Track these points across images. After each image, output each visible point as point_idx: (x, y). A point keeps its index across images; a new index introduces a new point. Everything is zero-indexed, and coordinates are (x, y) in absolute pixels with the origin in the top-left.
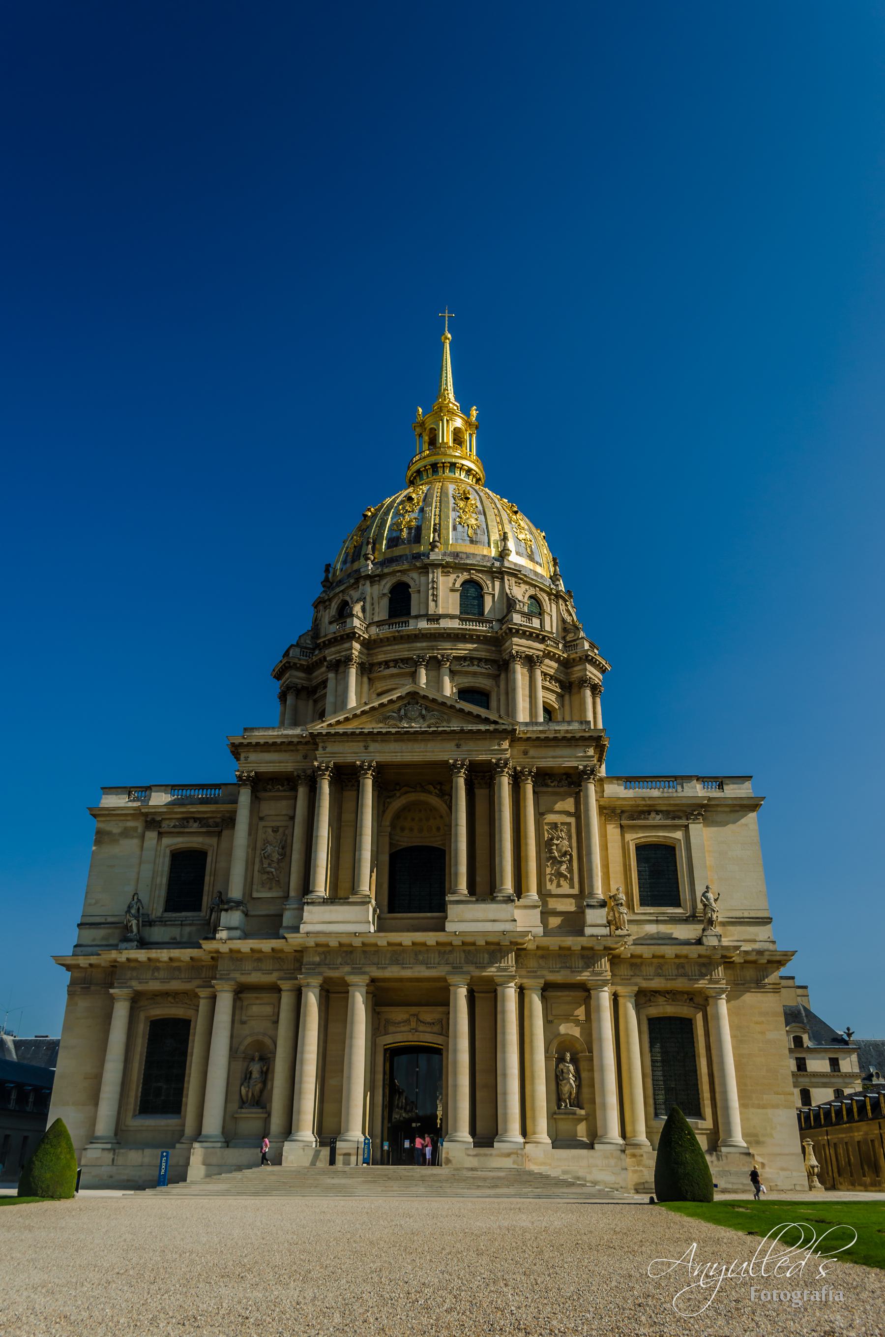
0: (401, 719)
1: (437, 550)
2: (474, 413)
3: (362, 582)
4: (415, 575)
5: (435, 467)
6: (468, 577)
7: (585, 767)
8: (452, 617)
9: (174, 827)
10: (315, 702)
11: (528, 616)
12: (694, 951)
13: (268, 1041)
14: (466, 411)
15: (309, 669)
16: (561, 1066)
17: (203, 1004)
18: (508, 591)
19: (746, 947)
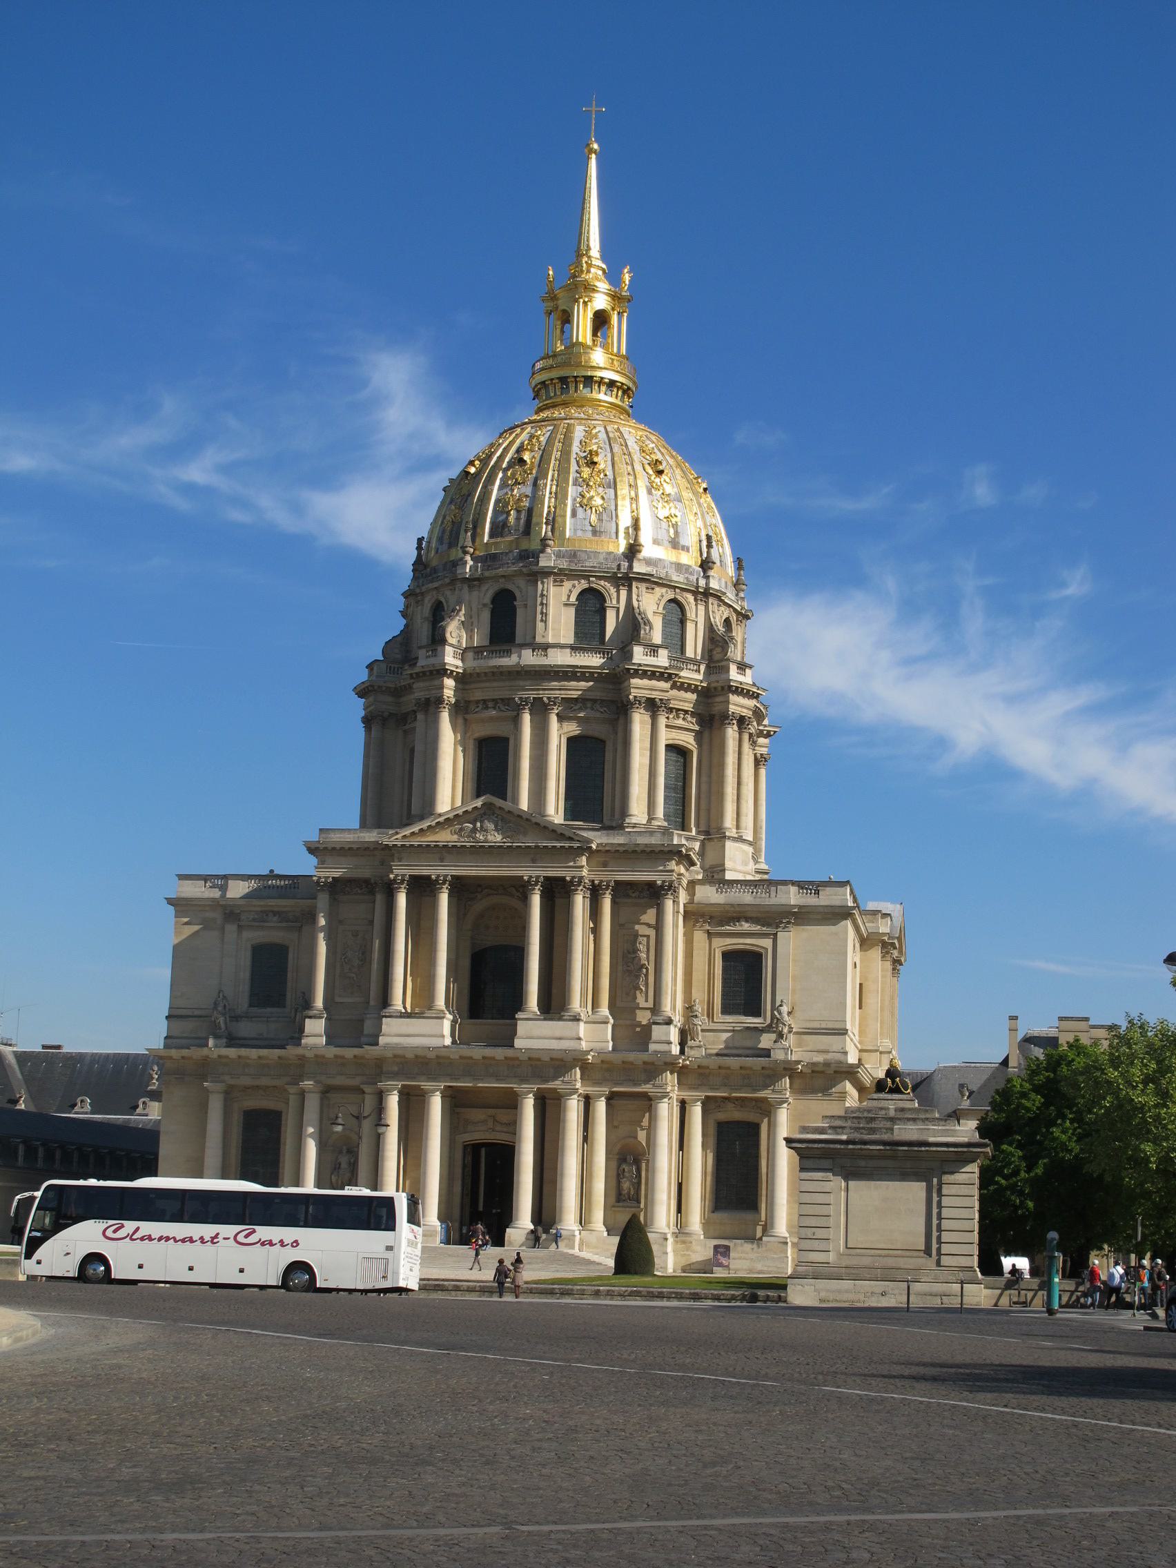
1: (549, 550)
2: (627, 278)
3: (459, 585)
5: (563, 380)
6: (586, 586)
7: (664, 882)
9: (254, 920)
11: (653, 649)
13: (355, 1137)
14: (613, 276)
15: (398, 692)
16: (624, 1166)
17: (293, 1100)
18: (635, 604)
19: (819, 1058)
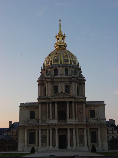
0: (60, 96)
4: (58, 67)
5: (59, 46)
8: (64, 75)
10: (44, 86)
12: (96, 124)
19: (103, 123)
